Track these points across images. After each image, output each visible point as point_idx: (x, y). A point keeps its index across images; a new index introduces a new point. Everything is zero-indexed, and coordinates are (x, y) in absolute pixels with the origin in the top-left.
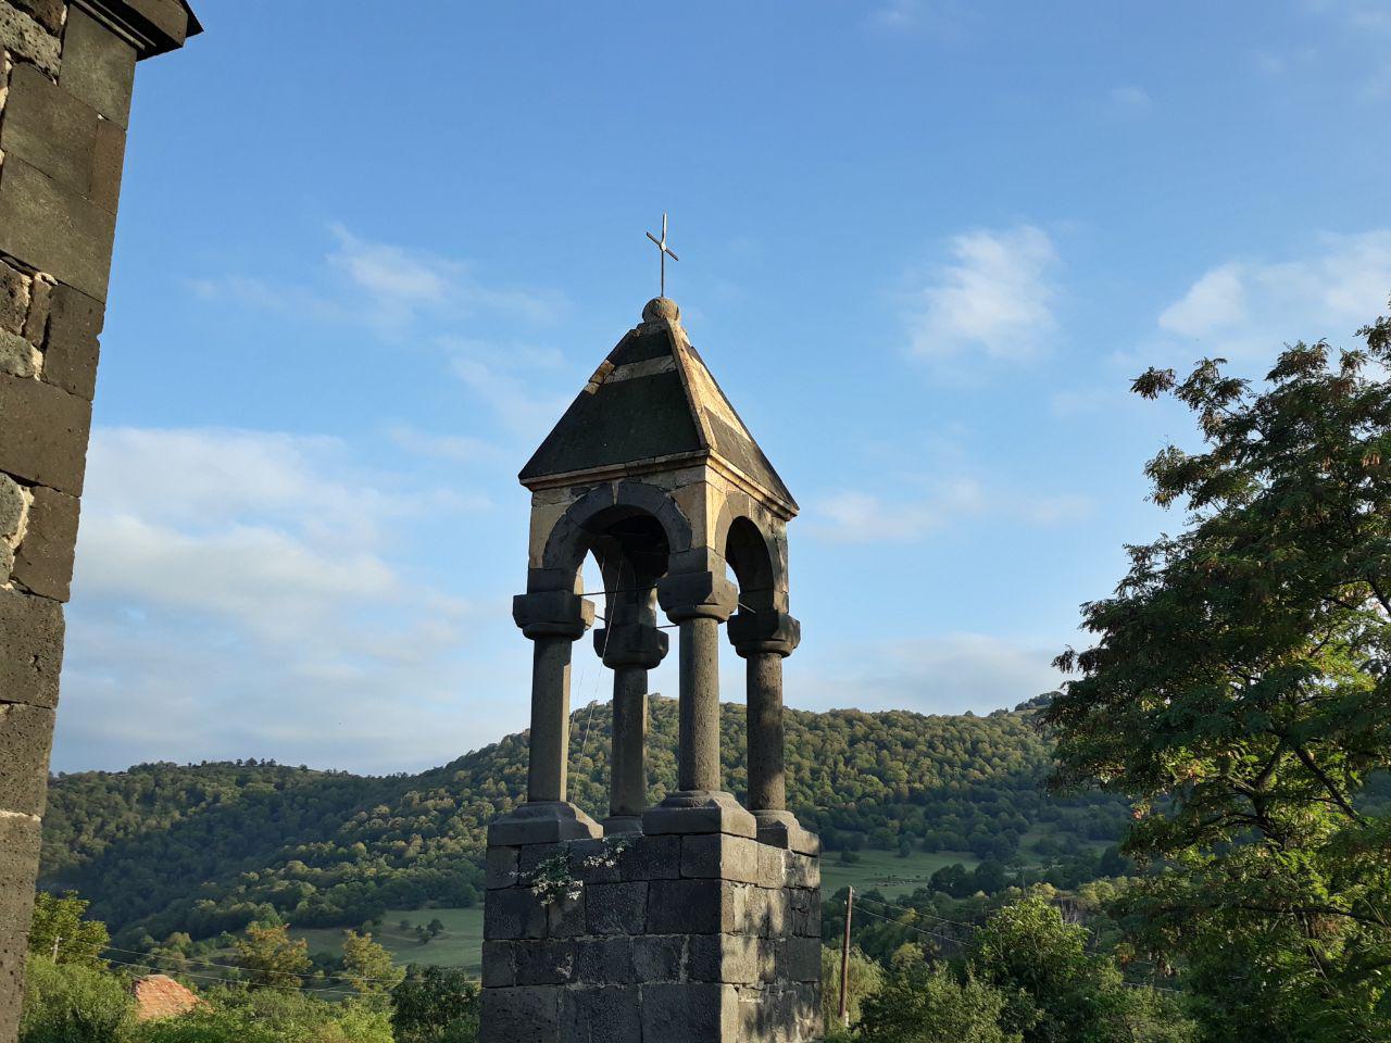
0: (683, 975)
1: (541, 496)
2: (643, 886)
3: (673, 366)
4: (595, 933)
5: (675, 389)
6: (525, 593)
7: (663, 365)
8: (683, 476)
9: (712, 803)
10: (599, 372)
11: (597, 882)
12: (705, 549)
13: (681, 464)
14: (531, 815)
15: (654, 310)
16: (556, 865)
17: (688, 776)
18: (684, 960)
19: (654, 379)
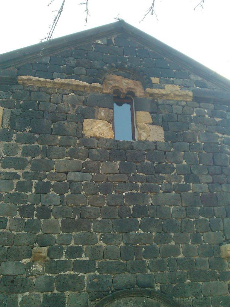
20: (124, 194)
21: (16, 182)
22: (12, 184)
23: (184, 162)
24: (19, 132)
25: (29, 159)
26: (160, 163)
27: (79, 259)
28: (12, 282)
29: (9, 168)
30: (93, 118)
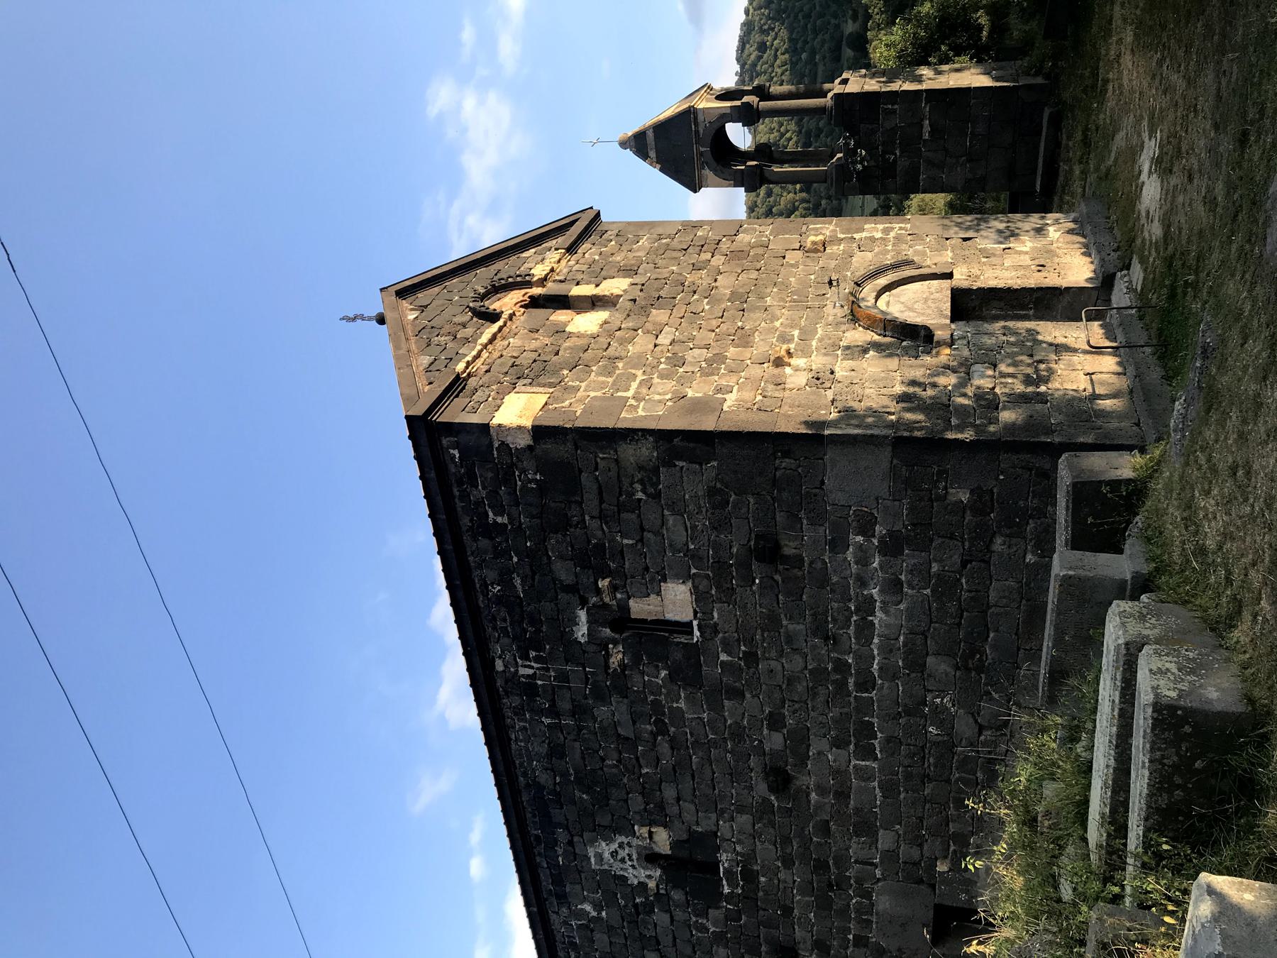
0: (896, 107)
1: (704, 184)
2: (862, 125)
3: (651, 130)
4: (878, 145)
5: (664, 129)
6: (743, 189)
7: (650, 134)
8: (701, 118)
9: (832, 98)
10: (651, 165)
11: (857, 145)
12: (731, 107)
13: (696, 118)
14: (832, 178)
15: (624, 144)
16: (852, 163)
17: (821, 110)
18: (890, 107)
19: (656, 137)
20: (707, 307)
21: (656, 380)
22: (658, 383)
23: (674, 268)
24: (566, 380)
25: (617, 372)
26: (666, 284)
27: (796, 336)
28: (818, 379)
29: (630, 386)
30: (566, 324)
